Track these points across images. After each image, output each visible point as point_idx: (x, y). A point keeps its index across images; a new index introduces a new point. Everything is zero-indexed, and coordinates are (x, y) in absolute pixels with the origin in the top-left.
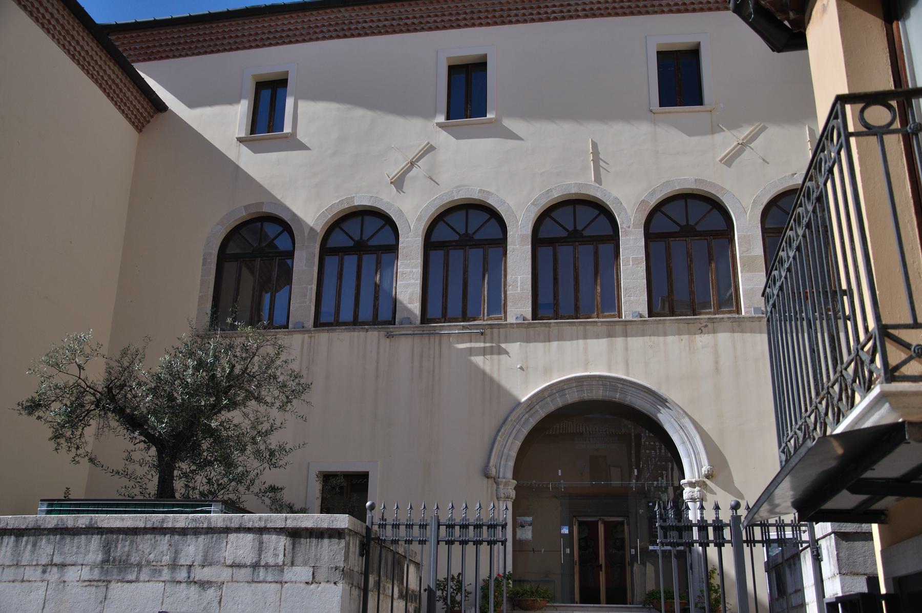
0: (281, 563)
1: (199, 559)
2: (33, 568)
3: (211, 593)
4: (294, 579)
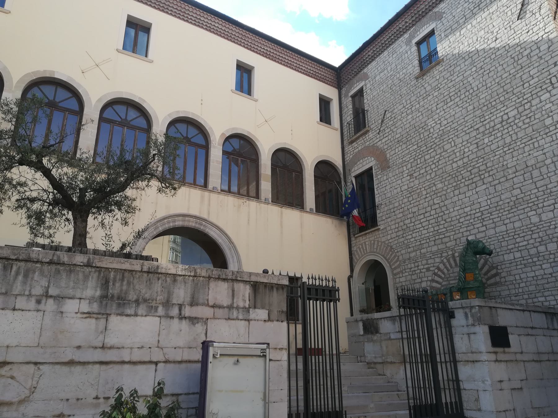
0: (247, 306)
1: (188, 299)
2: (25, 298)
3: (199, 328)
4: (257, 318)
